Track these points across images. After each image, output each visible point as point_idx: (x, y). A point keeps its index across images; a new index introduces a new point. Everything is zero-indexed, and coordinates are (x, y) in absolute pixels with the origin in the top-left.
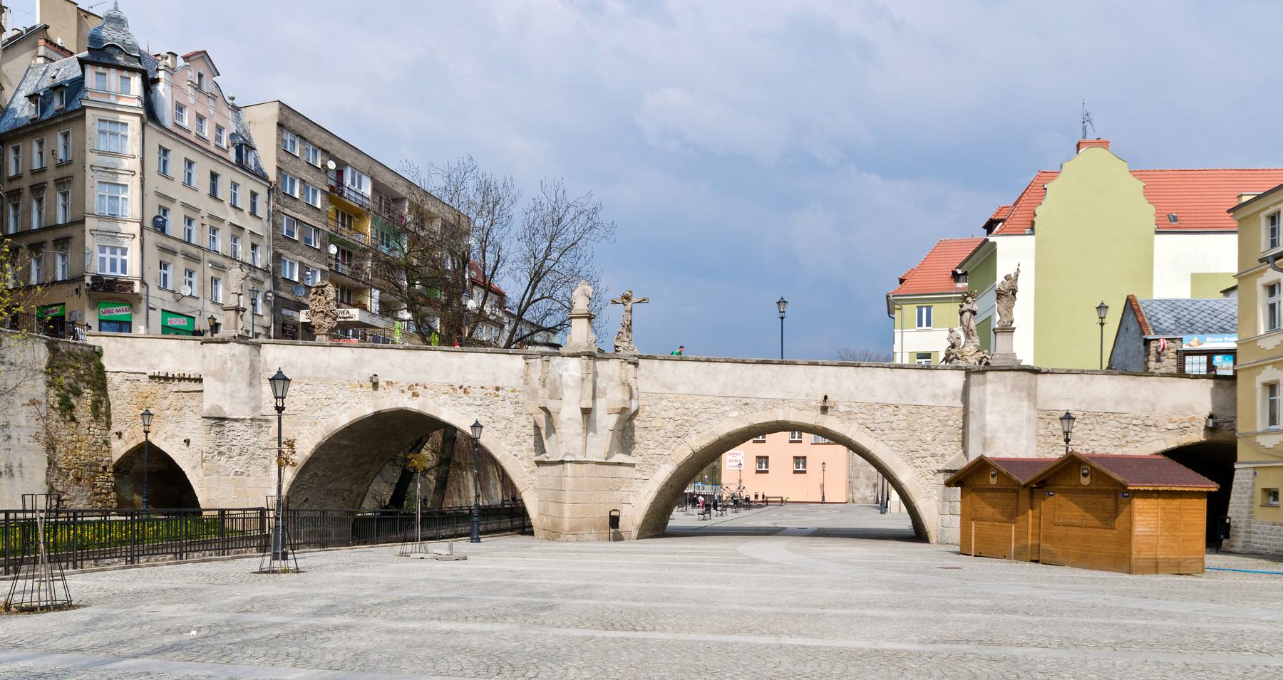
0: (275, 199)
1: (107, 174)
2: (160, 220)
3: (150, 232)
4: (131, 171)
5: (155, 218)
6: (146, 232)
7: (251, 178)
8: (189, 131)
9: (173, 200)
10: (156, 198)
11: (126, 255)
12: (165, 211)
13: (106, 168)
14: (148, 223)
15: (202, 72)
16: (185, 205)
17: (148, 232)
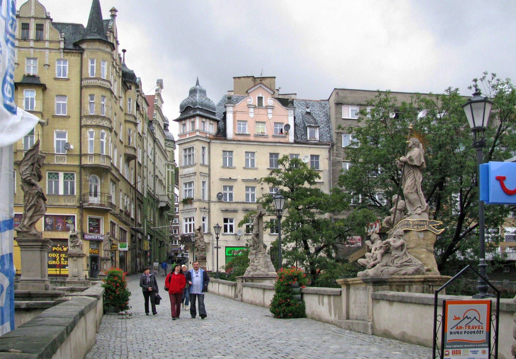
0: (335, 155)
1: (186, 178)
2: (221, 195)
3: (216, 203)
4: (194, 173)
5: (217, 195)
6: (212, 205)
7: (310, 148)
8: (249, 135)
9: (235, 180)
10: (221, 182)
11: (232, 222)
12: (231, 188)
13: (185, 175)
14: (214, 198)
15: (260, 95)
16: (243, 180)
17: (214, 204)
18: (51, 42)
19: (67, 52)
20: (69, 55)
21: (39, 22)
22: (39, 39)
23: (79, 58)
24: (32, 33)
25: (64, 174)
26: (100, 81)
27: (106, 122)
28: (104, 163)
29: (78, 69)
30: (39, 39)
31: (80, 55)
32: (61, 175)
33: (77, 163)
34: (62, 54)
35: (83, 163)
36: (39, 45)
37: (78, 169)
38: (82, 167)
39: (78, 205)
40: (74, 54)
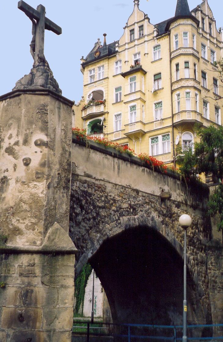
18: (148, 35)
19: (160, 38)
20: (161, 40)
21: (140, 24)
22: (142, 36)
23: (168, 39)
24: (137, 35)
25: (163, 136)
26: (182, 50)
27: (191, 82)
28: (190, 117)
29: (168, 48)
30: (142, 36)
31: (168, 37)
32: (160, 137)
33: (171, 124)
34: (156, 40)
35: (174, 122)
36: (142, 41)
37: (170, 129)
38: (174, 126)
39: (172, 160)
40: (164, 37)
